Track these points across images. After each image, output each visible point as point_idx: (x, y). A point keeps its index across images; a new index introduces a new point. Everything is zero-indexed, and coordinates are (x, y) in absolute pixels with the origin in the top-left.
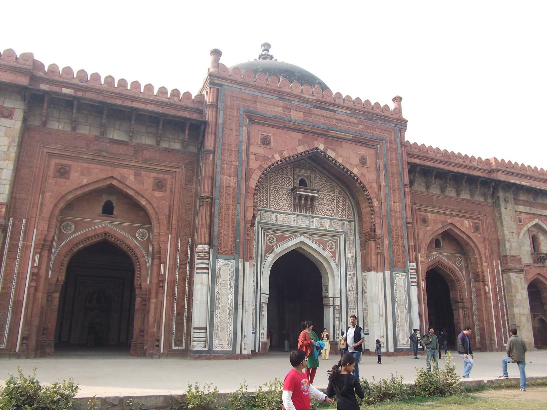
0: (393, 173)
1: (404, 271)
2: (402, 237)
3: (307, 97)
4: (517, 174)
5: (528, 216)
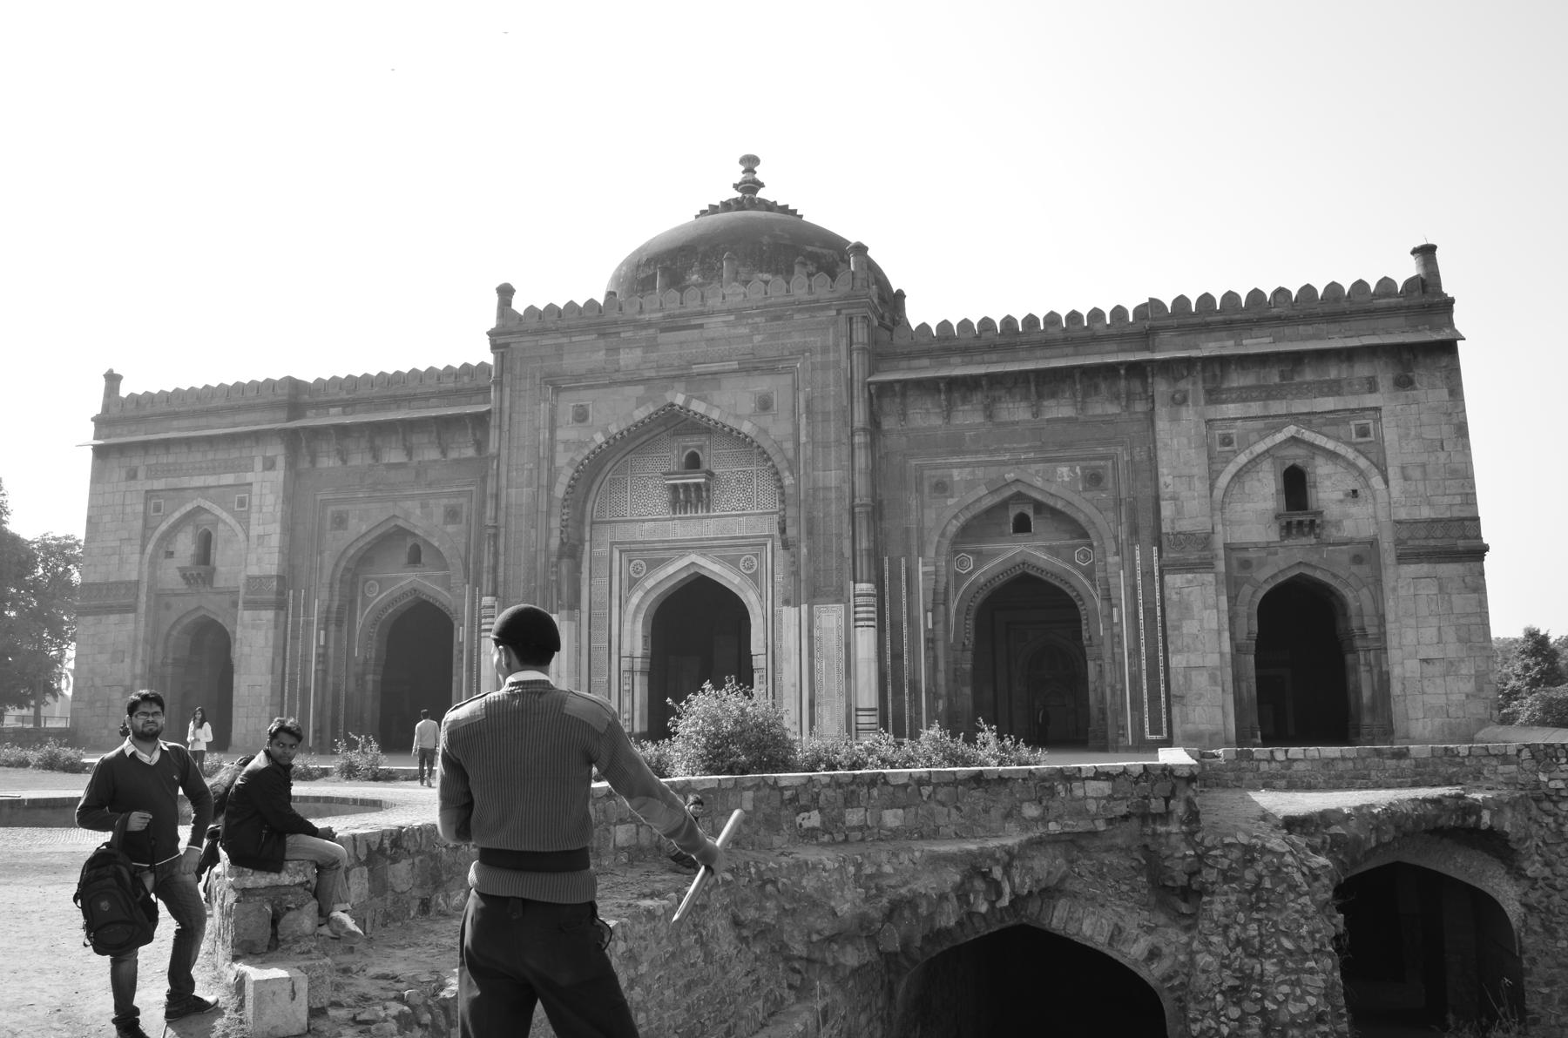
0: (826, 414)
1: (838, 601)
2: (839, 536)
3: (646, 317)
4: (1224, 322)
5: (1260, 424)
